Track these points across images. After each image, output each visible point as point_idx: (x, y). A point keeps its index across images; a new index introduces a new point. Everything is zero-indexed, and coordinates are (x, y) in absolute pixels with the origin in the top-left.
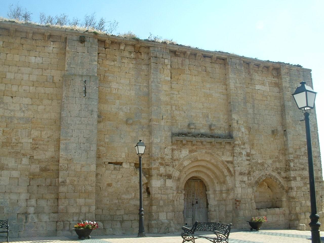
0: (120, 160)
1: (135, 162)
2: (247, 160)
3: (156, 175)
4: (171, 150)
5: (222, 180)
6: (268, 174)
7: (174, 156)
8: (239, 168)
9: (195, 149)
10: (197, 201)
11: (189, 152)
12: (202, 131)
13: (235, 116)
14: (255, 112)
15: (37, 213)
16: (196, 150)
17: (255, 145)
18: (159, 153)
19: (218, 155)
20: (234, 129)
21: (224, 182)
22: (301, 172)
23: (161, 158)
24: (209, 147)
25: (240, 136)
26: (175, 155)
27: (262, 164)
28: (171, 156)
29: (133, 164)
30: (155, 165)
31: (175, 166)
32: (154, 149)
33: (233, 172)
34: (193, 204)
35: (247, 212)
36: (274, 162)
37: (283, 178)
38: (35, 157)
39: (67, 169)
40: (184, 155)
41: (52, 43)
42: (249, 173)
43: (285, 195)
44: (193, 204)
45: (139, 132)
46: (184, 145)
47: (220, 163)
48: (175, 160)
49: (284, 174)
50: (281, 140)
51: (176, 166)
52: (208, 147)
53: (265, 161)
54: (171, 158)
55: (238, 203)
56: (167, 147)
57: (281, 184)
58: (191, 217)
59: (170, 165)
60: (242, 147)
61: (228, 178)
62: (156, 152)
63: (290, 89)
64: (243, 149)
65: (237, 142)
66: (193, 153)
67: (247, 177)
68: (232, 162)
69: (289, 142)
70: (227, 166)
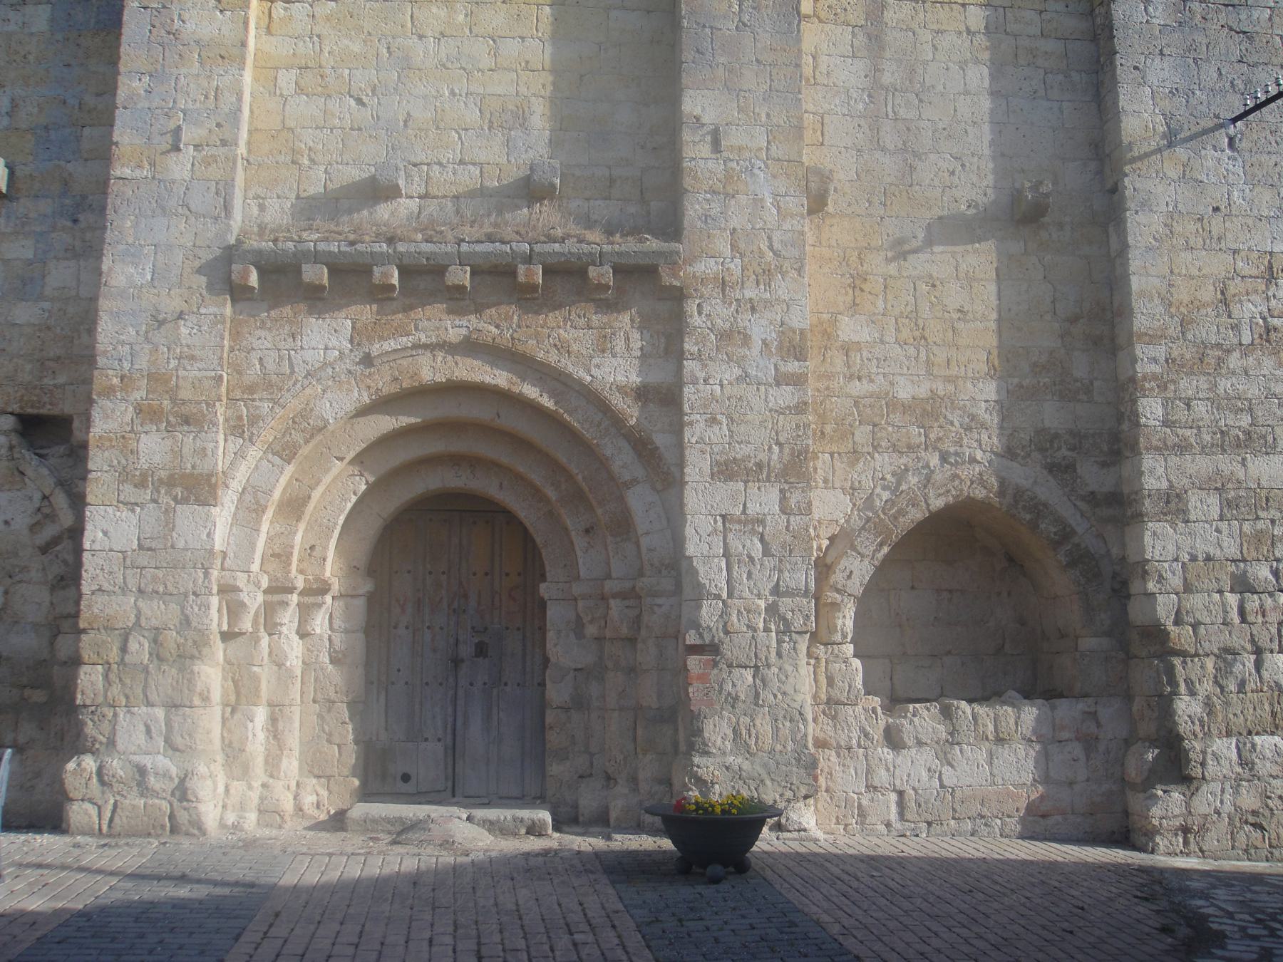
1: (15, 407)
8: (718, 435)
14: (887, 79)
18: (137, 348)
21: (623, 525)
22: (1228, 464)
23: (150, 377)
25: (735, 222)
34: (456, 662)
37: (1092, 498)
44: (456, 662)
45: (53, 235)
53: (951, 388)
57: (1076, 540)
58: (439, 740)
59: (204, 416)
62: (123, 343)
65: (705, 267)
66: (382, 338)
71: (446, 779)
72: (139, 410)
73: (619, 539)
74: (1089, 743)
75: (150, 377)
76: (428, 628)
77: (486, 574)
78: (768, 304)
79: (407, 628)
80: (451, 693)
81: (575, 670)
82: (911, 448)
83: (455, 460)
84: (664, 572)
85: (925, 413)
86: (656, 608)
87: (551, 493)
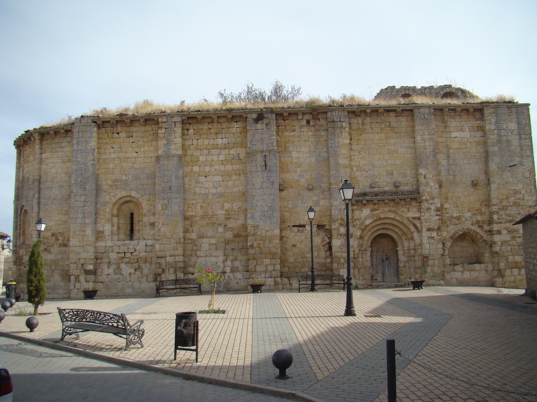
0: (303, 223)
2: (437, 215)
3: (336, 235)
5: (409, 237)
6: (466, 228)
8: (427, 224)
12: (387, 189)
13: (422, 171)
14: (450, 163)
15: (232, 271)
17: (450, 198)
19: (403, 212)
20: (421, 184)
21: (412, 238)
23: (341, 219)
25: (428, 190)
27: (459, 218)
29: (316, 226)
30: (335, 226)
32: (333, 211)
33: (420, 228)
35: (436, 268)
36: (474, 215)
37: (486, 231)
38: (229, 226)
39: (254, 235)
40: (365, 215)
41: (235, 124)
42: (439, 229)
43: (488, 251)
44: (383, 261)
46: (365, 205)
49: (486, 228)
50: (484, 190)
55: (425, 259)
60: (431, 202)
61: (415, 235)
63: (496, 132)
64: (431, 204)
65: (424, 198)
67: (436, 233)
68: (419, 219)
69: (492, 192)
72: (340, 224)
74: (487, 271)
75: (341, 219)
78: (434, 203)
82: (456, 224)
83: (383, 229)
85: (458, 219)
87: (400, 234)
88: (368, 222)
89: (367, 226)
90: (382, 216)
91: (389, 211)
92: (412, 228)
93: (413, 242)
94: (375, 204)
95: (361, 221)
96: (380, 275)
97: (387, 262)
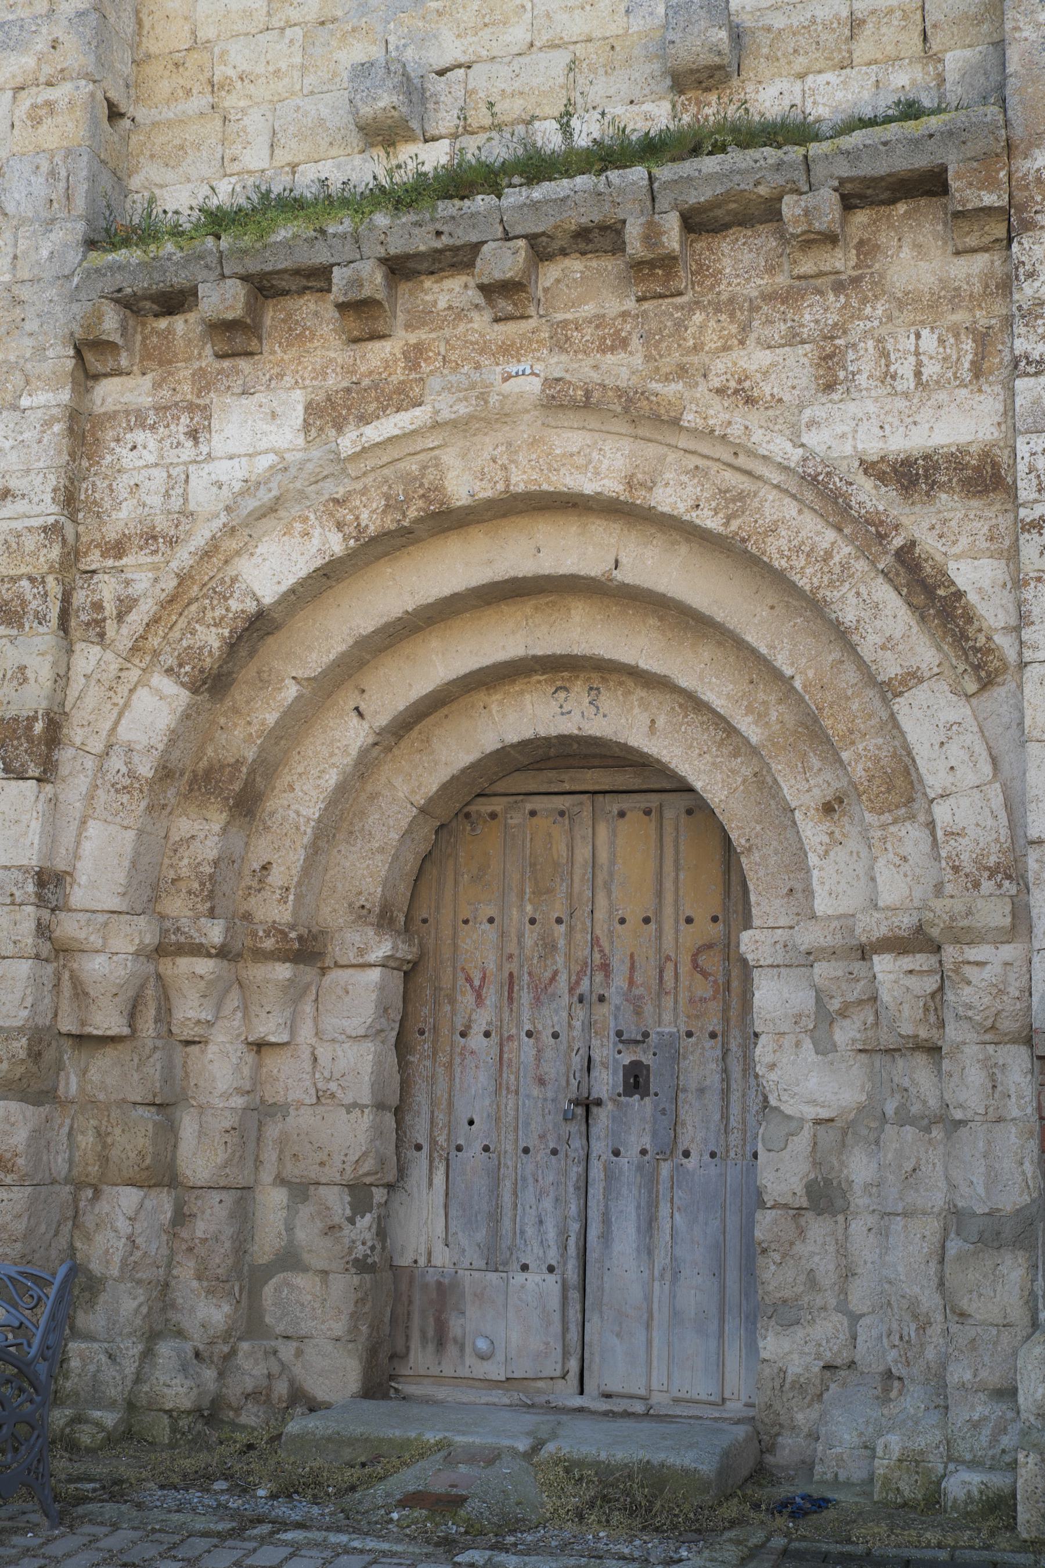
4: (57, 428)
5: (861, 756)
7: (107, 505)
9: (399, 375)
10: (647, 1059)
11: (307, 426)
16: (401, 389)
21: (901, 786)
24: (599, 321)
26: (123, 483)
28: (48, 497)
31: (120, 617)
33: (992, 613)
34: (588, 1105)
40: (232, 473)
47: (790, 509)
48: (118, 549)
51: (133, 617)
52: (589, 309)
54: (45, 529)
56: (15, 407)
58: (551, 1269)
59: (24, 603)
61: (936, 723)
66: (364, 419)
70: (898, 542)
71: (566, 1354)
73: (887, 817)
76: (529, 1034)
77: (647, 920)
79: (487, 1034)
80: (576, 1170)
81: (818, 1122)
84: (987, 886)
86: (969, 971)
88: (270, 570)
89: (258, 628)
90: (462, 487)
91: (563, 402)
92: (883, 618)
93: (912, 837)
94: (363, 317)
95: (183, 557)
96: (538, 1288)
97: (635, 1125)
